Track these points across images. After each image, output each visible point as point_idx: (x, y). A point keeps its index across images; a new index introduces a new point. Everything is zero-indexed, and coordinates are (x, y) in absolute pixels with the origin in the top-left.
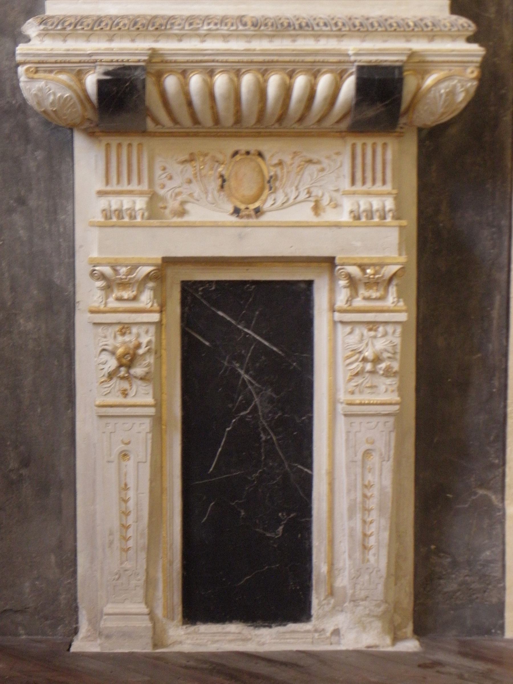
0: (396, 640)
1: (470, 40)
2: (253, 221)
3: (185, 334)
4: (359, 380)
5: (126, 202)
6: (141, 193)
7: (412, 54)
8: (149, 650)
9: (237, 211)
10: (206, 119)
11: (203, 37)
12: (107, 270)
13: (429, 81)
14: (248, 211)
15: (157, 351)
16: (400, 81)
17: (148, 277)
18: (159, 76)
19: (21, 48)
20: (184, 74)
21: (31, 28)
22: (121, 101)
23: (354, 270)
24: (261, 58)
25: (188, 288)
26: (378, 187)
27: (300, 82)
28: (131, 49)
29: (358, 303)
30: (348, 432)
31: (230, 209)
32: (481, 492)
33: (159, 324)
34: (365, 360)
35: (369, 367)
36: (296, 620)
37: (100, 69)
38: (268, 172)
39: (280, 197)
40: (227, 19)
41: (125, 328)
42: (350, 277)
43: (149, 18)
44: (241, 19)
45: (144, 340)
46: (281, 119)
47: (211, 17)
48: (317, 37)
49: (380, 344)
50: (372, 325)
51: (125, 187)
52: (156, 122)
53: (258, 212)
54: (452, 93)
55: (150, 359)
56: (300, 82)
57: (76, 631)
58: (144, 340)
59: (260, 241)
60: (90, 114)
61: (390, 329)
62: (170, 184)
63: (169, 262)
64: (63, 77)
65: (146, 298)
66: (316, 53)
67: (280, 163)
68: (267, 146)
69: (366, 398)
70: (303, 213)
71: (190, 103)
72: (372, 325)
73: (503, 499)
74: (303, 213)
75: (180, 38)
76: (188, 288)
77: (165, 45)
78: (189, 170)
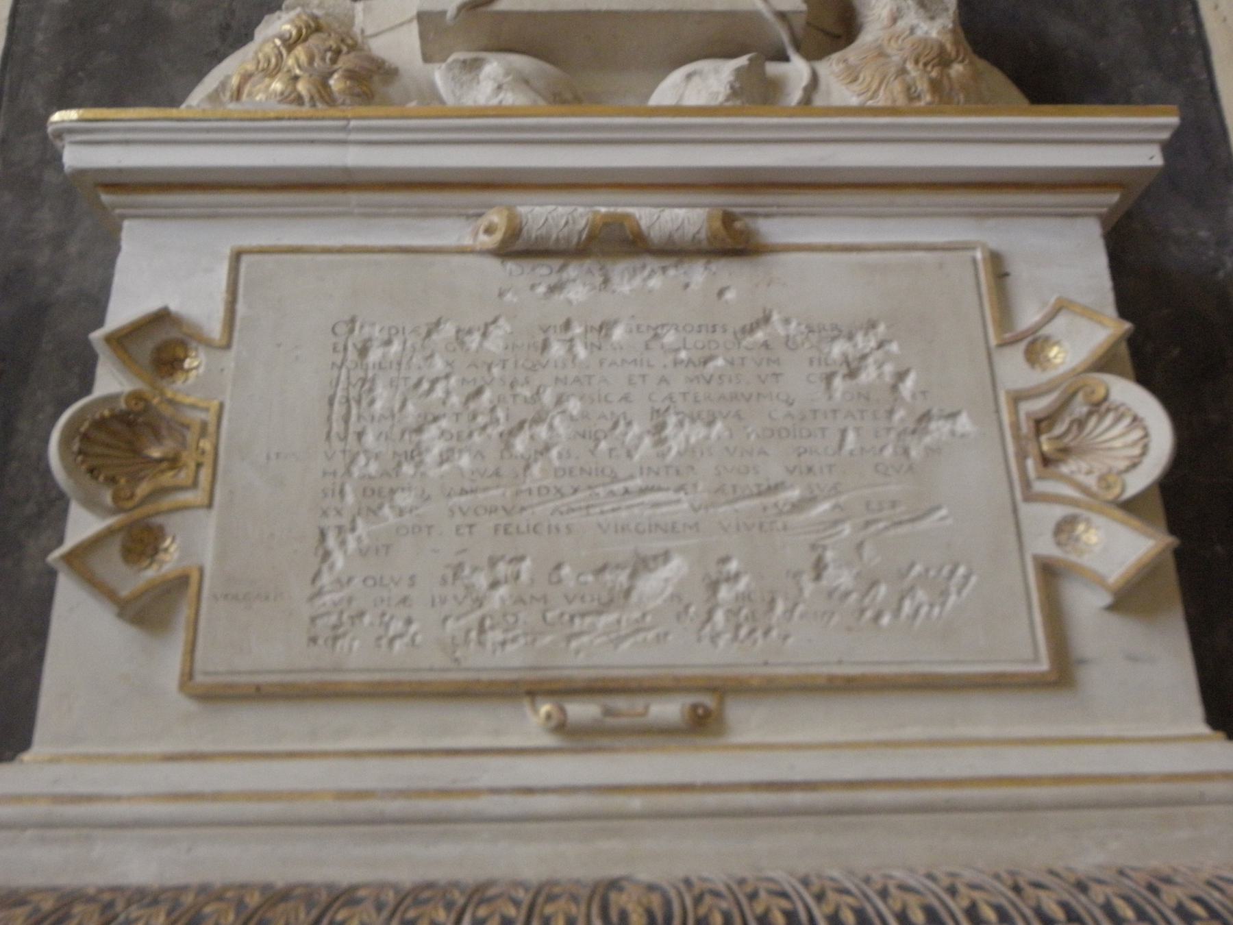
40: (551, 898)
43: (253, 900)
47: (491, 892)
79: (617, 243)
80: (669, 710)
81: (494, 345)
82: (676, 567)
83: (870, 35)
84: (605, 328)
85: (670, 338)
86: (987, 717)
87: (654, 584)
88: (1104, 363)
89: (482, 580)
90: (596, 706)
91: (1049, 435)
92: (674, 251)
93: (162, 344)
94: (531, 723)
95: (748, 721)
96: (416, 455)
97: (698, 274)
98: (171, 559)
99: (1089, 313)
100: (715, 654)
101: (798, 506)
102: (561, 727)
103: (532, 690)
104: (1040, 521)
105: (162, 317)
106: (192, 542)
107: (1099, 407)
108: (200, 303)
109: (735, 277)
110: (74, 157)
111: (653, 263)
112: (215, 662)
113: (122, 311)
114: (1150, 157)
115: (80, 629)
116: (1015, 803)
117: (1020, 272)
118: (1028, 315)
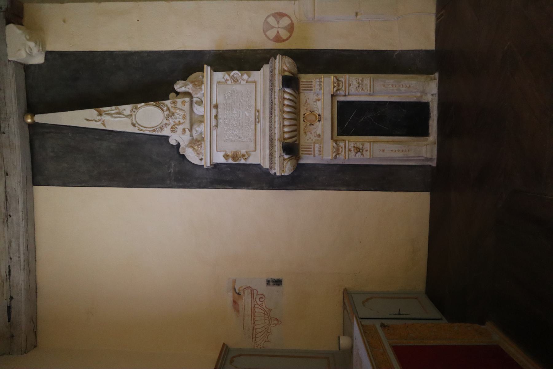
0: (435, 79)
1: (276, 59)
2: (322, 116)
3: (351, 135)
4: (364, 88)
5: (317, 149)
6: (314, 145)
7: (279, 73)
8: (436, 145)
9: (319, 121)
11: (275, 128)
12: (334, 154)
13: (286, 69)
14: (319, 118)
16: (286, 76)
17: (336, 143)
18: (285, 139)
19: (278, 174)
20: (284, 132)
21: (272, 172)
22: (291, 149)
23: (335, 89)
25: (339, 134)
26: (313, 83)
27: (286, 102)
28: (278, 147)
29: (343, 88)
31: (318, 123)
32: (394, 57)
34: (359, 86)
36: (429, 106)
37: (283, 154)
38: (308, 113)
39: (316, 109)
41: (350, 150)
42: (337, 91)
44: (270, 118)
45: (352, 145)
46: (295, 108)
48: (275, 98)
49: (355, 83)
50: (350, 85)
51: (313, 149)
52: (296, 141)
53: (319, 115)
54: (289, 63)
55: (358, 144)
56: (286, 102)
57: (430, 166)
59: (327, 115)
60: (294, 157)
61: (350, 80)
62: (312, 138)
63: (332, 138)
64: (285, 164)
65: (342, 144)
66: (279, 99)
67: (306, 109)
68: (302, 112)
69: (369, 87)
71: (292, 131)
72: (350, 85)
73: (397, 51)
74: (319, 104)
75: (275, 134)
76: (339, 134)
77: (277, 138)
78: (308, 133)
79: (216, 116)
80: (257, 114)
81: (226, 128)
82: (246, 113)
83: (191, 91)
86: (258, 89)
87: (247, 115)
88: (229, 75)
90: (257, 121)
91: (236, 81)
92: (217, 112)
93: (226, 156)
94: (258, 125)
95: (258, 108)
97: (219, 110)
98: (244, 153)
102: (258, 122)
103: (256, 125)
104: (242, 82)
105: (224, 156)
106: (243, 152)
108: (223, 153)
109: (219, 106)
110: (209, 165)
112: (253, 149)
113: (223, 160)
114: (209, 68)
115: (251, 161)
116: (264, 88)
117: (219, 80)
118: (223, 80)
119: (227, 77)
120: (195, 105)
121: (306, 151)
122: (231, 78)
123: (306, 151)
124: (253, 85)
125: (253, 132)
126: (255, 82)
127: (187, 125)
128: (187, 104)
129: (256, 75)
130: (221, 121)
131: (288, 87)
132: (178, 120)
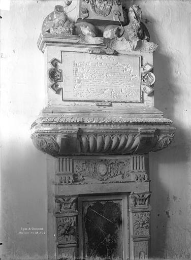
10: (85, 150)
15: (77, 224)
24: (112, 131)
30: (134, 247)
33: (77, 216)
35: (141, 226)
58: (73, 221)
61: (146, 213)
70: (119, 178)
84: (101, 63)
85: (108, 65)
89: (90, 91)
91: (143, 78)
96: (83, 77)
98: (59, 87)
99: (150, 65)
100: (112, 99)
101: (120, 84)
107: (150, 75)
111: (106, 56)
117: (144, 58)
119: (148, 68)
120: (116, 28)
121: (138, 161)
122: (146, 73)
123: (138, 161)
124: (139, 100)
125: (85, 99)
126: (143, 102)
127: (93, 16)
128: (115, 18)
129: (150, 101)
130: (98, 59)
131: (142, 140)
132: (98, 5)
